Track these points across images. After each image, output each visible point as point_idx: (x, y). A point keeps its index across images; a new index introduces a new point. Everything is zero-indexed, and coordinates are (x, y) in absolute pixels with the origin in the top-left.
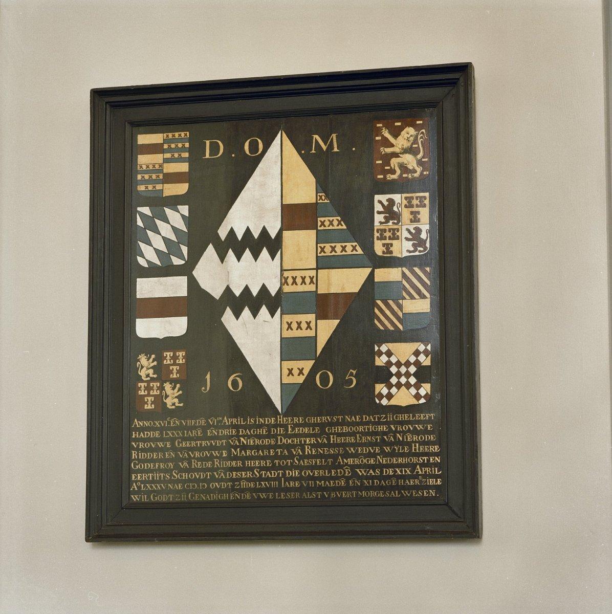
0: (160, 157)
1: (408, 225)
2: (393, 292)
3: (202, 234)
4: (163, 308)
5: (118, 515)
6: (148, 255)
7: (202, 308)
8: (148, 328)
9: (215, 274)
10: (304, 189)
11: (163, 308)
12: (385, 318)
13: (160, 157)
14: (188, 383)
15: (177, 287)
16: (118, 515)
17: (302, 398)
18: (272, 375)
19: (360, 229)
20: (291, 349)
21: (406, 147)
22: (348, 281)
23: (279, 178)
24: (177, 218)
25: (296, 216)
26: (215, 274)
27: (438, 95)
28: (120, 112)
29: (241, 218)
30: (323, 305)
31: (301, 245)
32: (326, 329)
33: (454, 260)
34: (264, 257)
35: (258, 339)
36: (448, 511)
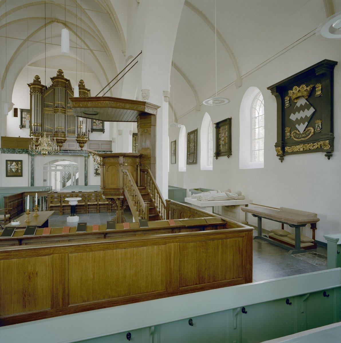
0: (9, 162)
1: (20, 166)
2: (19, 168)
3: (11, 165)
4: (9, 168)
5: (7, 176)
6: (8, 166)
7: (11, 168)
8: (8, 169)
10: (15, 164)
11: (9, 168)
12: (19, 169)
13: (9, 162)
14: (10, 171)
15: (10, 167)
16: (7, 176)
17: (15, 172)
18: (14, 171)
19: (18, 166)
20: (15, 170)
21: (20, 163)
22: (17, 168)
23: (14, 163)
24: (10, 165)
25: (15, 165)
27: (21, 161)
28: (7, 161)
29: (12, 165)
30: (16, 168)
32: (16, 169)
34: (13, 167)
35: (13, 170)
36: (21, 176)
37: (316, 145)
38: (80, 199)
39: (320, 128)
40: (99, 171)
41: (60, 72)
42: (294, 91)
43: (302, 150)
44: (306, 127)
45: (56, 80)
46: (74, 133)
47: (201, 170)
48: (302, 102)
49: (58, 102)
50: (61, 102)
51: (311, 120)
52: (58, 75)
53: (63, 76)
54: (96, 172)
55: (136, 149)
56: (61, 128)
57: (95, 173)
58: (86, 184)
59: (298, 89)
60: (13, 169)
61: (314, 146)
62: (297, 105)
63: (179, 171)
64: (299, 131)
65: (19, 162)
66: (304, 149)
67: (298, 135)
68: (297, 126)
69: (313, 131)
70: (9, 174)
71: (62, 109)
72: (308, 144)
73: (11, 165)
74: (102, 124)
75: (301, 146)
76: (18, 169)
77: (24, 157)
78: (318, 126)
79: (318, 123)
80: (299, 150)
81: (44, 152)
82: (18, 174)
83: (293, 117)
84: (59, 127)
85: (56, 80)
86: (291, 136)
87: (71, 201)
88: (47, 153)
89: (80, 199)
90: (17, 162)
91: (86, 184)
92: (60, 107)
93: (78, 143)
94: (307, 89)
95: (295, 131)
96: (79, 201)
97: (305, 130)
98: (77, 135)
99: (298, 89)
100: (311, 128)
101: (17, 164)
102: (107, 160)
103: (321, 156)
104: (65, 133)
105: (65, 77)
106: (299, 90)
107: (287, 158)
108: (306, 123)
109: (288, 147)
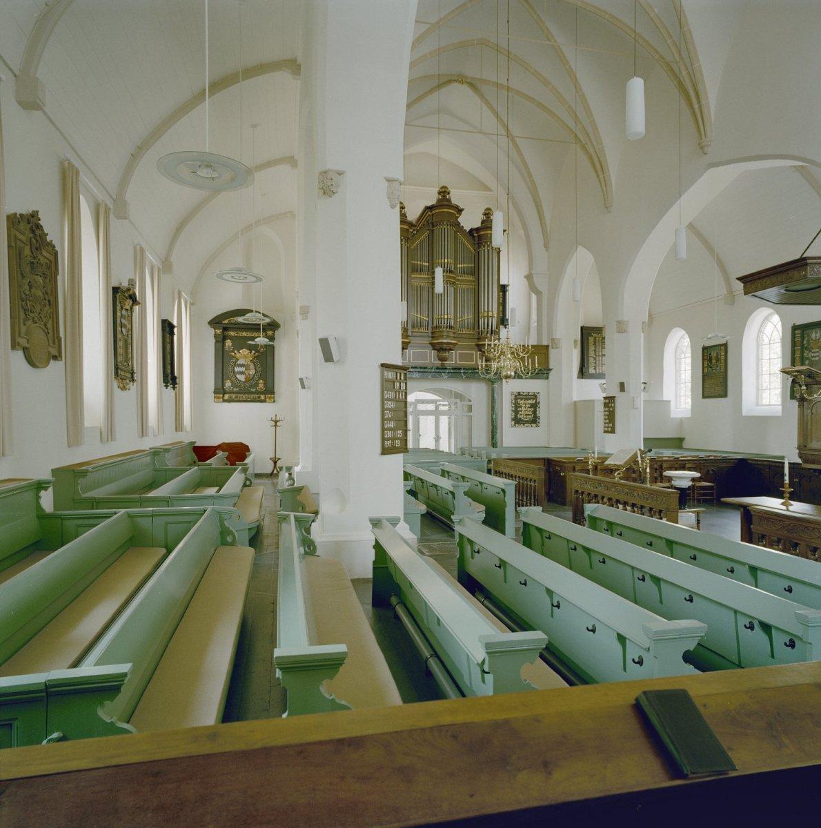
38: (696, 474)
40: (521, 415)
41: (444, 192)
45: (437, 211)
47: (744, 414)
49: (443, 261)
50: (446, 261)
52: (439, 201)
53: (449, 200)
54: (516, 416)
55: (595, 363)
56: (446, 317)
57: (513, 419)
63: (744, 414)
71: (448, 274)
81: (509, 373)
84: (446, 317)
85: (437, 211)
87: (675, 477)
88: (513, 374)
89: (696, 474)
96: (693, 480)
105: (454, 201)
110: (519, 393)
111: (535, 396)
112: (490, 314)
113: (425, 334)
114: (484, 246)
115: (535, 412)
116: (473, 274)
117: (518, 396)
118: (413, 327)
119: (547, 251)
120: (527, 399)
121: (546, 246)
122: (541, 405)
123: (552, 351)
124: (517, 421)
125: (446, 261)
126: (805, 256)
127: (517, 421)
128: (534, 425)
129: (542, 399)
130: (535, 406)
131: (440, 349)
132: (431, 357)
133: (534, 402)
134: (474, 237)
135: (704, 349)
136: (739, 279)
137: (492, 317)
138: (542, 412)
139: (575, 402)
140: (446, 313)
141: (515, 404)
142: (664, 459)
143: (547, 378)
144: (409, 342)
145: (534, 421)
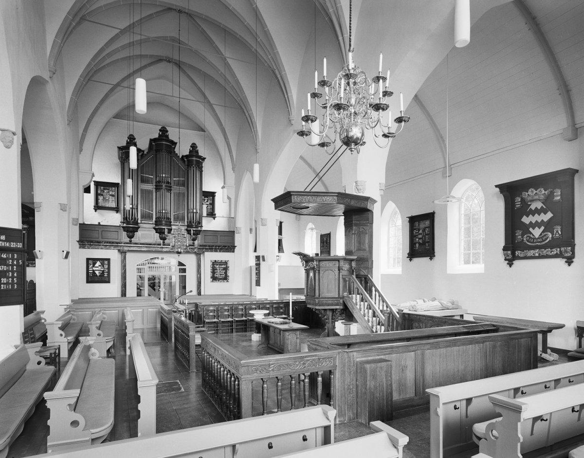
0: (90, 262)
1: (106, 267)
3: (93, 266)
5: (88, 282)
6: (90, 267)
7: (93, 271)
9: (94, 269)
10: (100, 264)
14: (92, 274)
16: (88, 282)
17: (100, 276)
18: (98, 274)
19: (103, 267)
21: (106, 262)
22: (103, 269)
23: (98, 264)
24: (92, 265)
25: (99, 266)
26: (94, 269)
27: (108, 260)
28: (88, 259)
29: (96, 266)
30: (101, 271)
31: (100, 267)
33: (109, 268)
35: (97, 272)
36: (109, 282)
37: (555, 251)
39: (559, 234)
42: (530, 193)
43: (537, 255)
44: (543, 232)
46: (183, 219)
48: (539, 205)
51: (548, 226)
56: (164, 211)
57: (211, 277)
58: (199, 293)
59: (535, 192)
60: (96, 272)
61: (552, 251)
62: (530, 207)
64: (533, 235)
65: (106, 261)
66: (539, 254)
67: (532, 239)
68: (531, 229)
69: (551, 236)
70: (92, 278)
72: (545, 249)
73: (93, 266)
74: (211, 206)
75: (536, 252)
76: (103, 271)
77: (112, 254)
78: (557, 232)
79: (558, 229)
80: (533, 255)
82: (104, 278)
83: (526, 220)
84: (164, 211)
86: (523, 240)
90: (102, 260)
91: (199, 293)
92: (163, 181)
93: (156, 232)
94: (545, 193)
95: (529, 235)
97: (541, 234)
98: (188, 222)
99: (535, 192)
100: (549, 234)
101: (103, 265)
102: (323, 264)
103: (560, 262)
104: (171, 219)
106: (536, 193)
107: (516, 263)
108: (543, 228)
109: (520, 252)
110: (215, 261)
111: (226, 263)
112: (195, 211)
113: (151, 222)
114: (193, 167)
115: (226, 273)
116: (184, 185)
117: (214, 263)
118: (142, 217)
119: (234, 172)
120: (221, 265)
121: (233, 169)
122: (230, 268)
123: (236, 236)
124: (214, 278)
125: (164, 175)
126: (306, 190)
127: (214, 278)
128: (225, 281)
129: (230, 264)
130: (226, 269)
131: (160, 232)
132: (155, 237)
133: (225, 266)
134: (184, 161)
135: (322, 236)
136: (272, 200)
137: (196, 213)
138: (230, 273)
139: (251, 267)
140: (195, 208)
141: (213, 268)
142: (274, 302)
143: (233, 252)
144: (139, 227)
145: (226, 278)
